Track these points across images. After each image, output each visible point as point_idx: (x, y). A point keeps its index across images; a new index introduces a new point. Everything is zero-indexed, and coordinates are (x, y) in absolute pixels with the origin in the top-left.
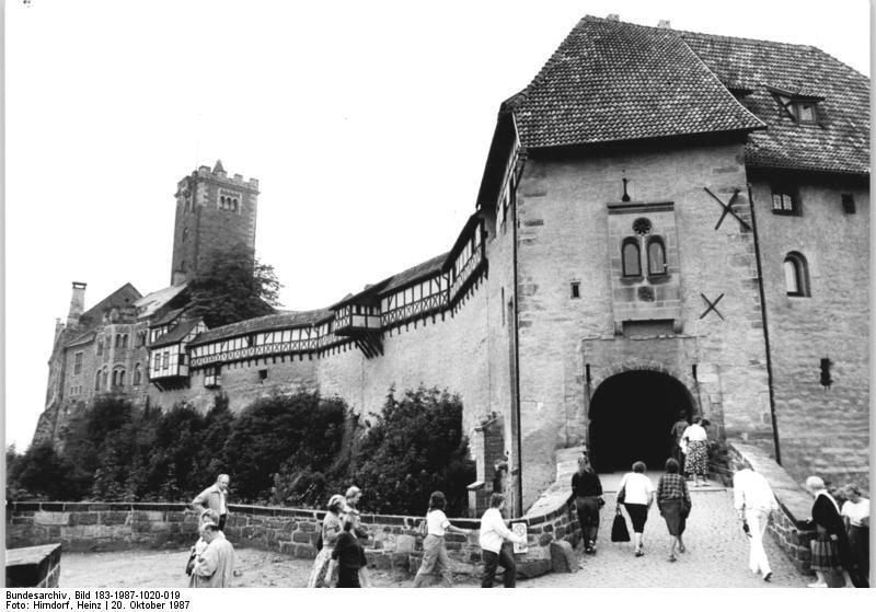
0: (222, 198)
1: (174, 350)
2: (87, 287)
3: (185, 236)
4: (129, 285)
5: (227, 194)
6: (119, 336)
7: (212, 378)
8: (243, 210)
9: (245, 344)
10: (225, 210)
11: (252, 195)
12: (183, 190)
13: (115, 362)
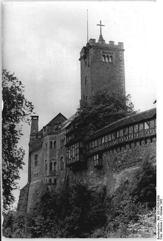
0: (104, 56)
1: (76, 146)
2: (38, 118)
3: (86, 81)
4: (60, 113)
5: (106, 53)
6: (51, 142)
7: (97, 161)
8: (116, 61)
9: (113, 138)
10: (106, 63)
11: (120, 52)
12: (82, 55)
13: (50, 157)
